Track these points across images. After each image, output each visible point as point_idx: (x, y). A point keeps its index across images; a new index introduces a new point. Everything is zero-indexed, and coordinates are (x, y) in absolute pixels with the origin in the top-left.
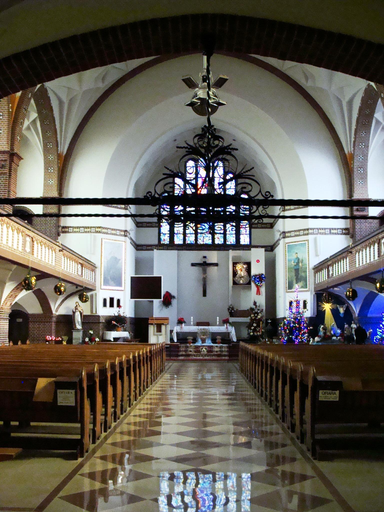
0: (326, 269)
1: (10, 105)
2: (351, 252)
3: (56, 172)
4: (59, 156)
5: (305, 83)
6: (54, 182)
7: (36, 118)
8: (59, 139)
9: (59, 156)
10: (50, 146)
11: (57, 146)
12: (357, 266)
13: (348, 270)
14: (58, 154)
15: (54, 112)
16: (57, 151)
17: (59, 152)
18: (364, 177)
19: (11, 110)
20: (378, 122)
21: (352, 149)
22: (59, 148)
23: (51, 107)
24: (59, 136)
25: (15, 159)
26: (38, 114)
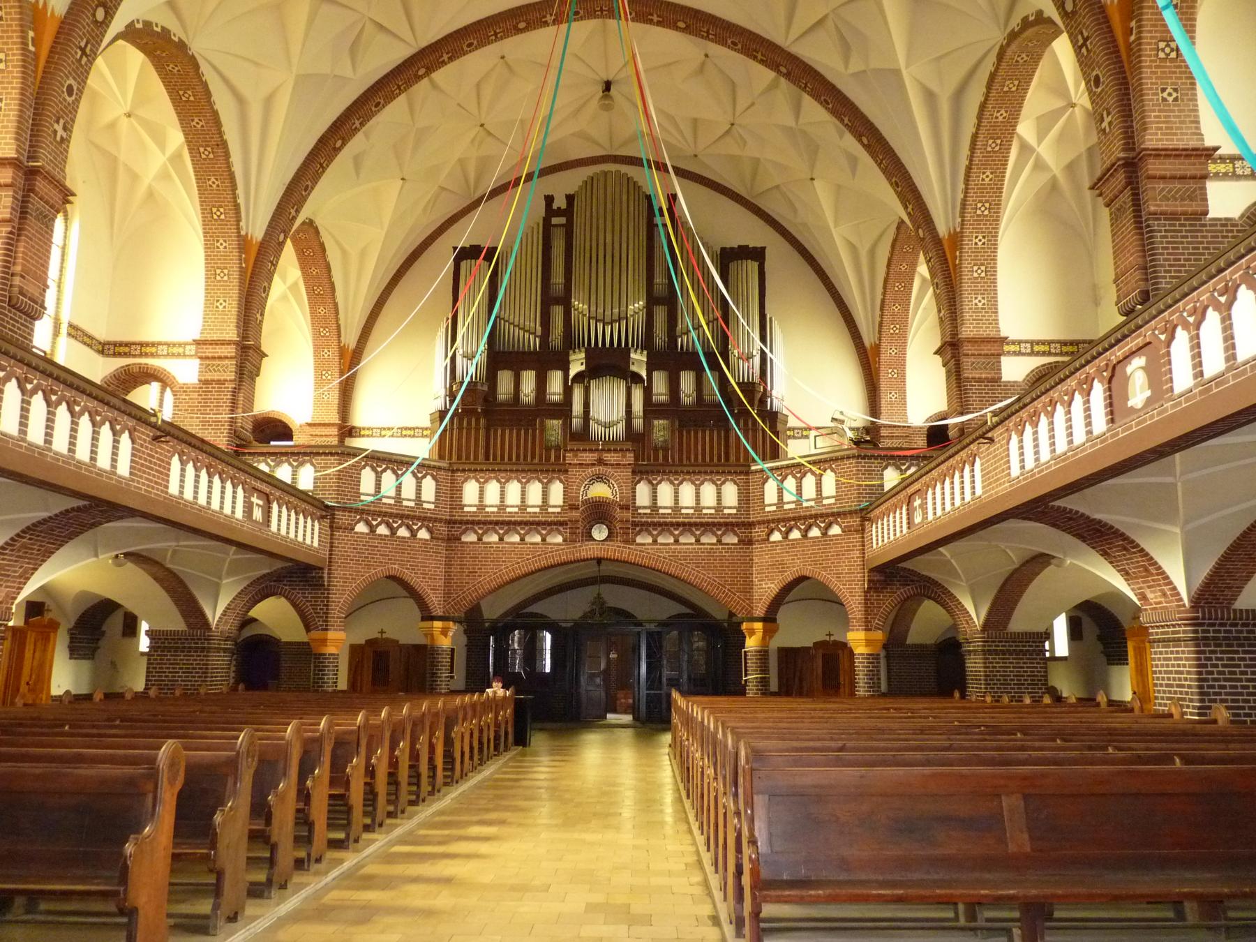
0: (905, 508)
1: (31, 34)
2: (991, 440)
3: (236, 282)
4: (243, 243)
5: (840, 67)
6: (230, 306)
7: (181, 147)
8: (241, 201)
9: (243, 243)
10: (220, 213)
11: (238, 220)
12: (1015, 471)
13: (979, 492)
14: (239, 236)
15: (225, 128)
16: (238, 229)
17: (243, 233)
18: (989, 286)
19: (32, 48)
20: (1025, 148)
21: (959, 220)
22: (242, 224)
23: (215, 114)
24: (240, 191)
25: (41, 185)
26: (186, 135)
